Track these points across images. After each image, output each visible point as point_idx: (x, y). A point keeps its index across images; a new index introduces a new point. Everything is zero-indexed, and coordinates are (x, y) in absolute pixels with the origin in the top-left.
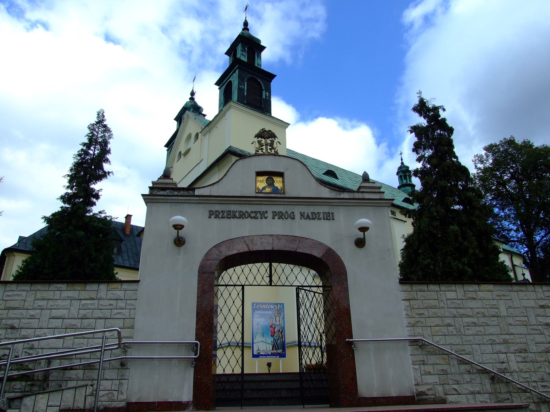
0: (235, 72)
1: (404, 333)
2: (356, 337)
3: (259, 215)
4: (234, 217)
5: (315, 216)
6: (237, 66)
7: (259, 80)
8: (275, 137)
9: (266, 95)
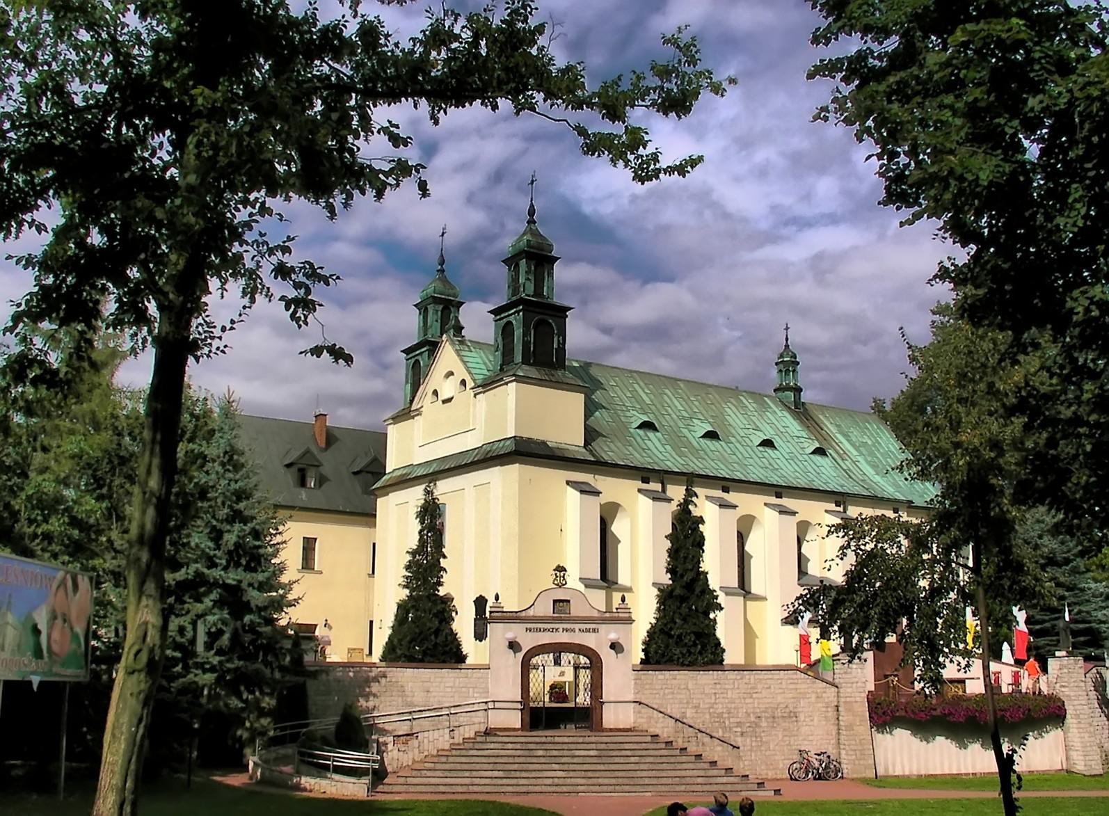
0: (518, 312)
1: (631, 697)
5: (588, 631)
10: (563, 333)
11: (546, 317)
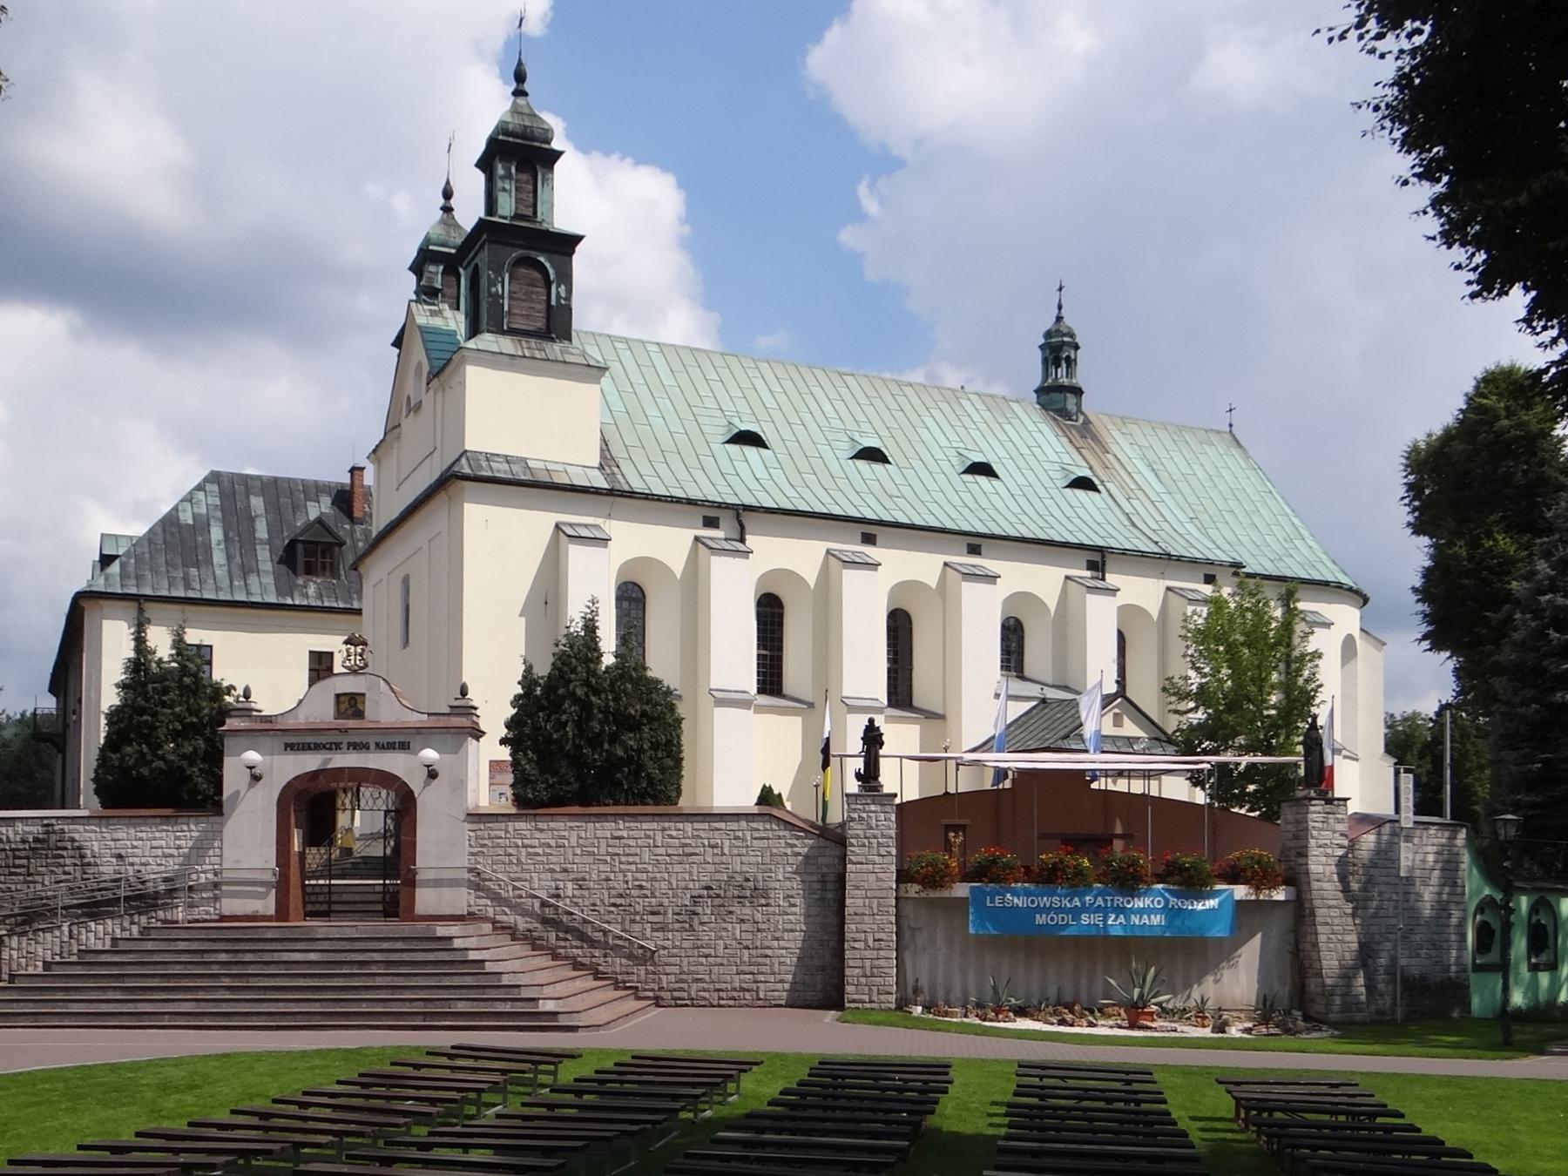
0: (482, 247)
2: (419, 864)
3: (334, 746)
4: (309, 748)
6: (485, 236)
7: (542, 259)
8: (366, 644)
9: (558, 293)
10: (566, 277)
11: (533, 253)
